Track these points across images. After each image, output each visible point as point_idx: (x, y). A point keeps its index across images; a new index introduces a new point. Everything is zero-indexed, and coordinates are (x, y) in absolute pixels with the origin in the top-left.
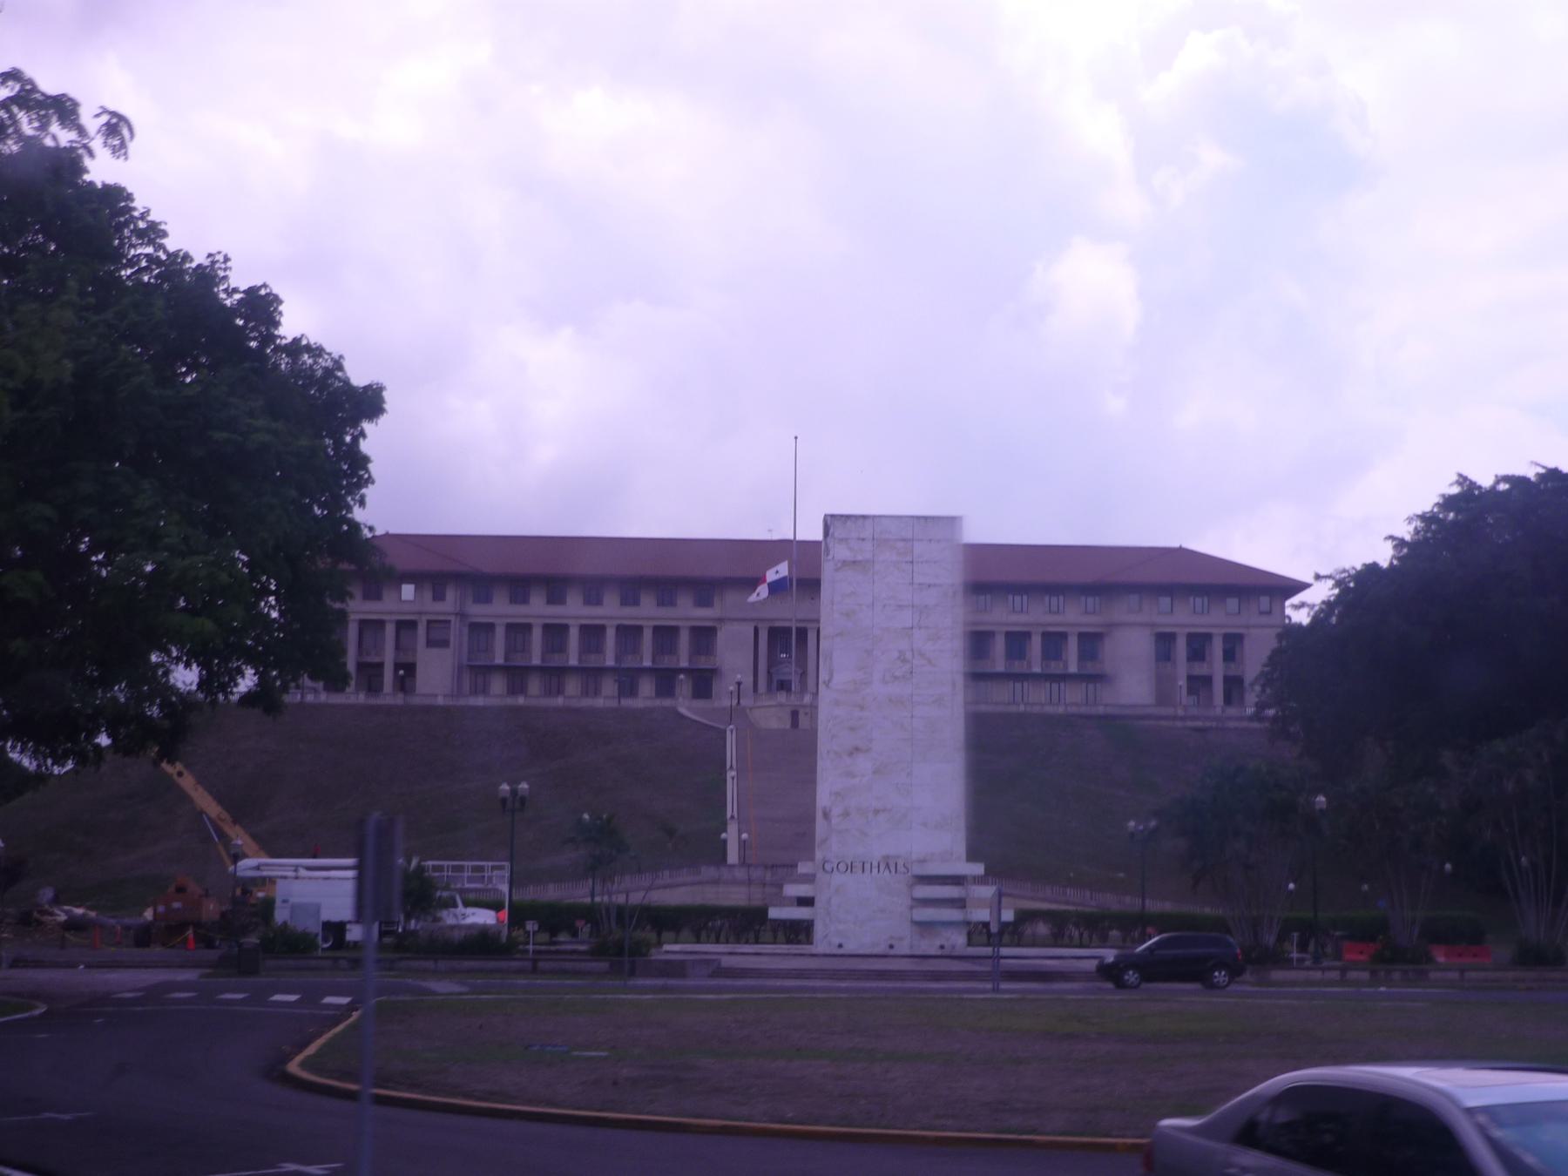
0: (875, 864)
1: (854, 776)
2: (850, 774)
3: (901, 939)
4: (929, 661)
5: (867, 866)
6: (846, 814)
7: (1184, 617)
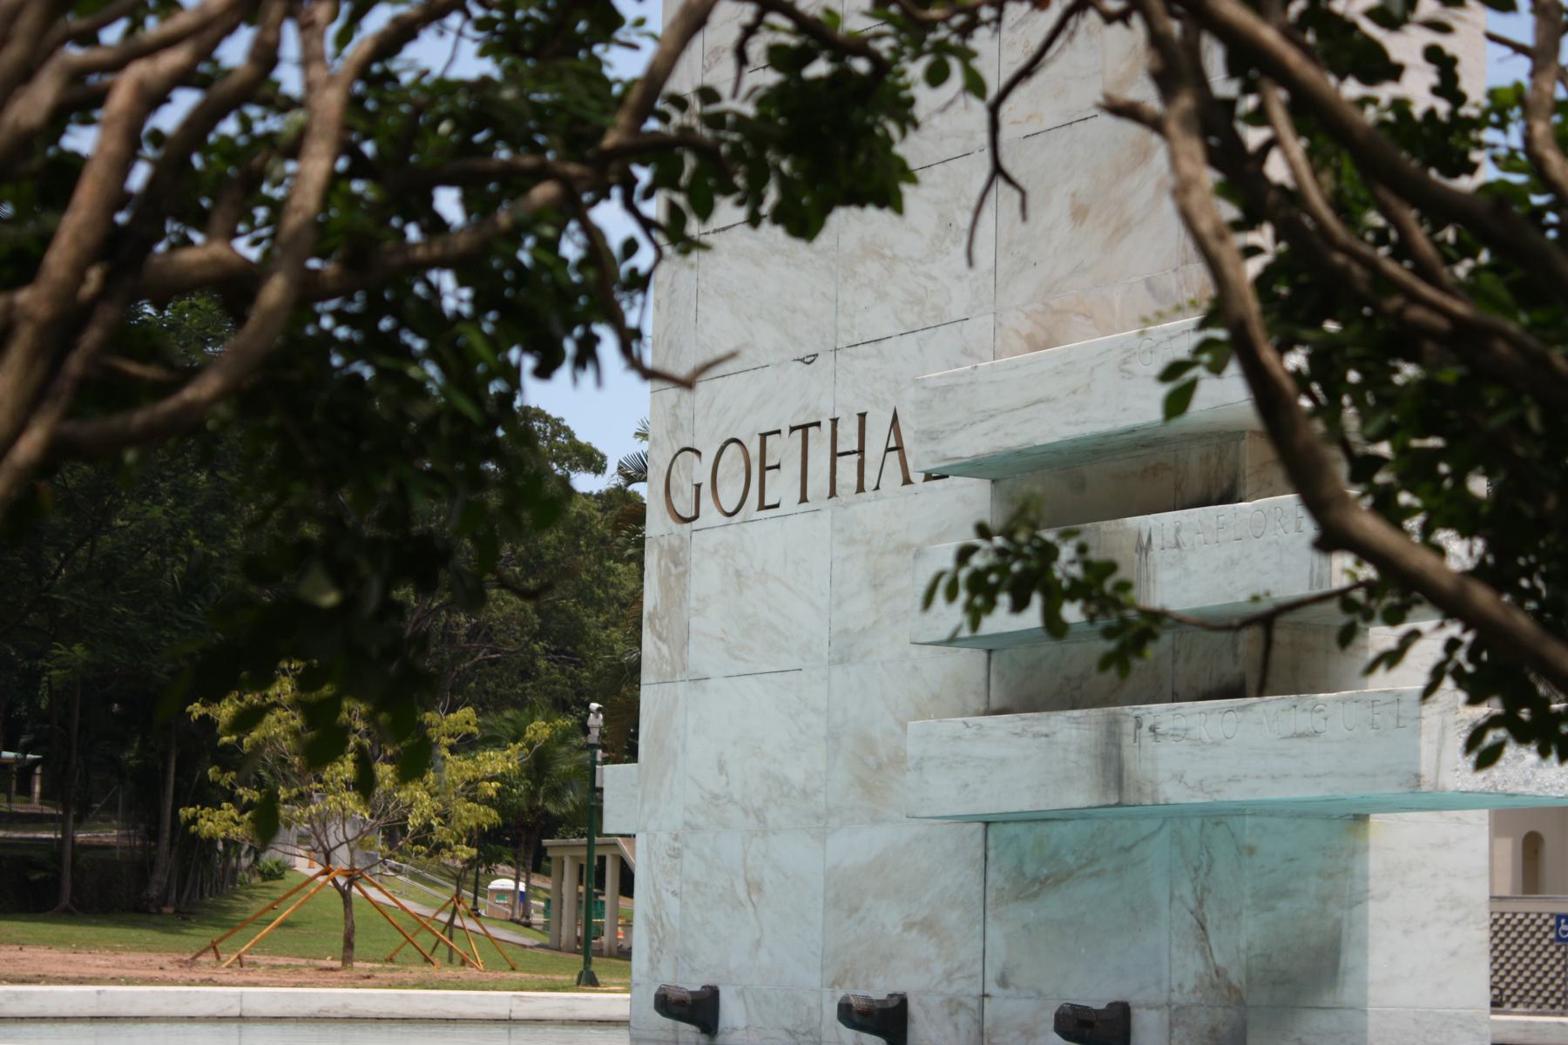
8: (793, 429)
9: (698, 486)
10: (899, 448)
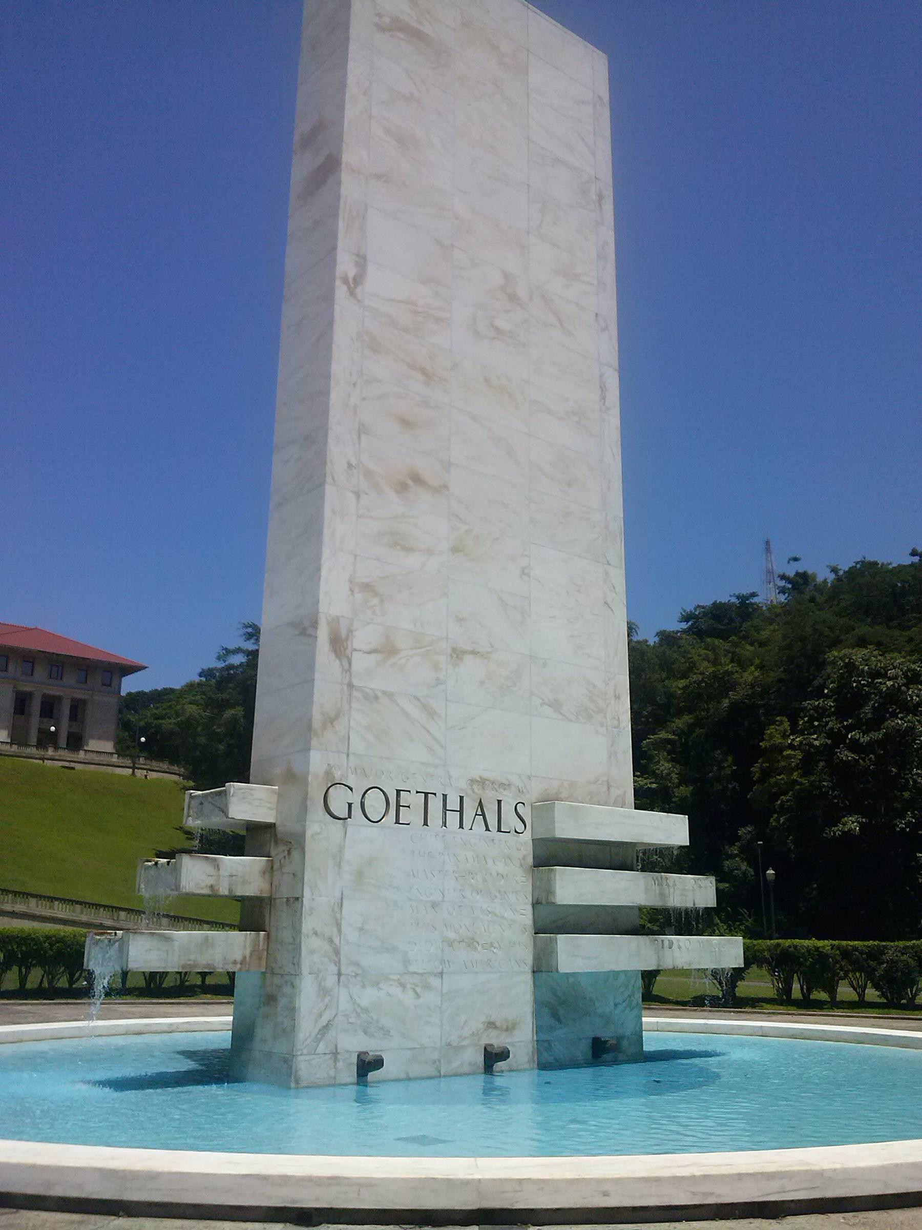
0: (453, 804)
1: (408, 550)
2: (399, 542)
3: (510, 1028)
4: (560, 321)
5: (435, 804)
6: (387, 650)
7: (39, 684)
8: (417, 792)
9: (350, 805)
10: (483, 815)
